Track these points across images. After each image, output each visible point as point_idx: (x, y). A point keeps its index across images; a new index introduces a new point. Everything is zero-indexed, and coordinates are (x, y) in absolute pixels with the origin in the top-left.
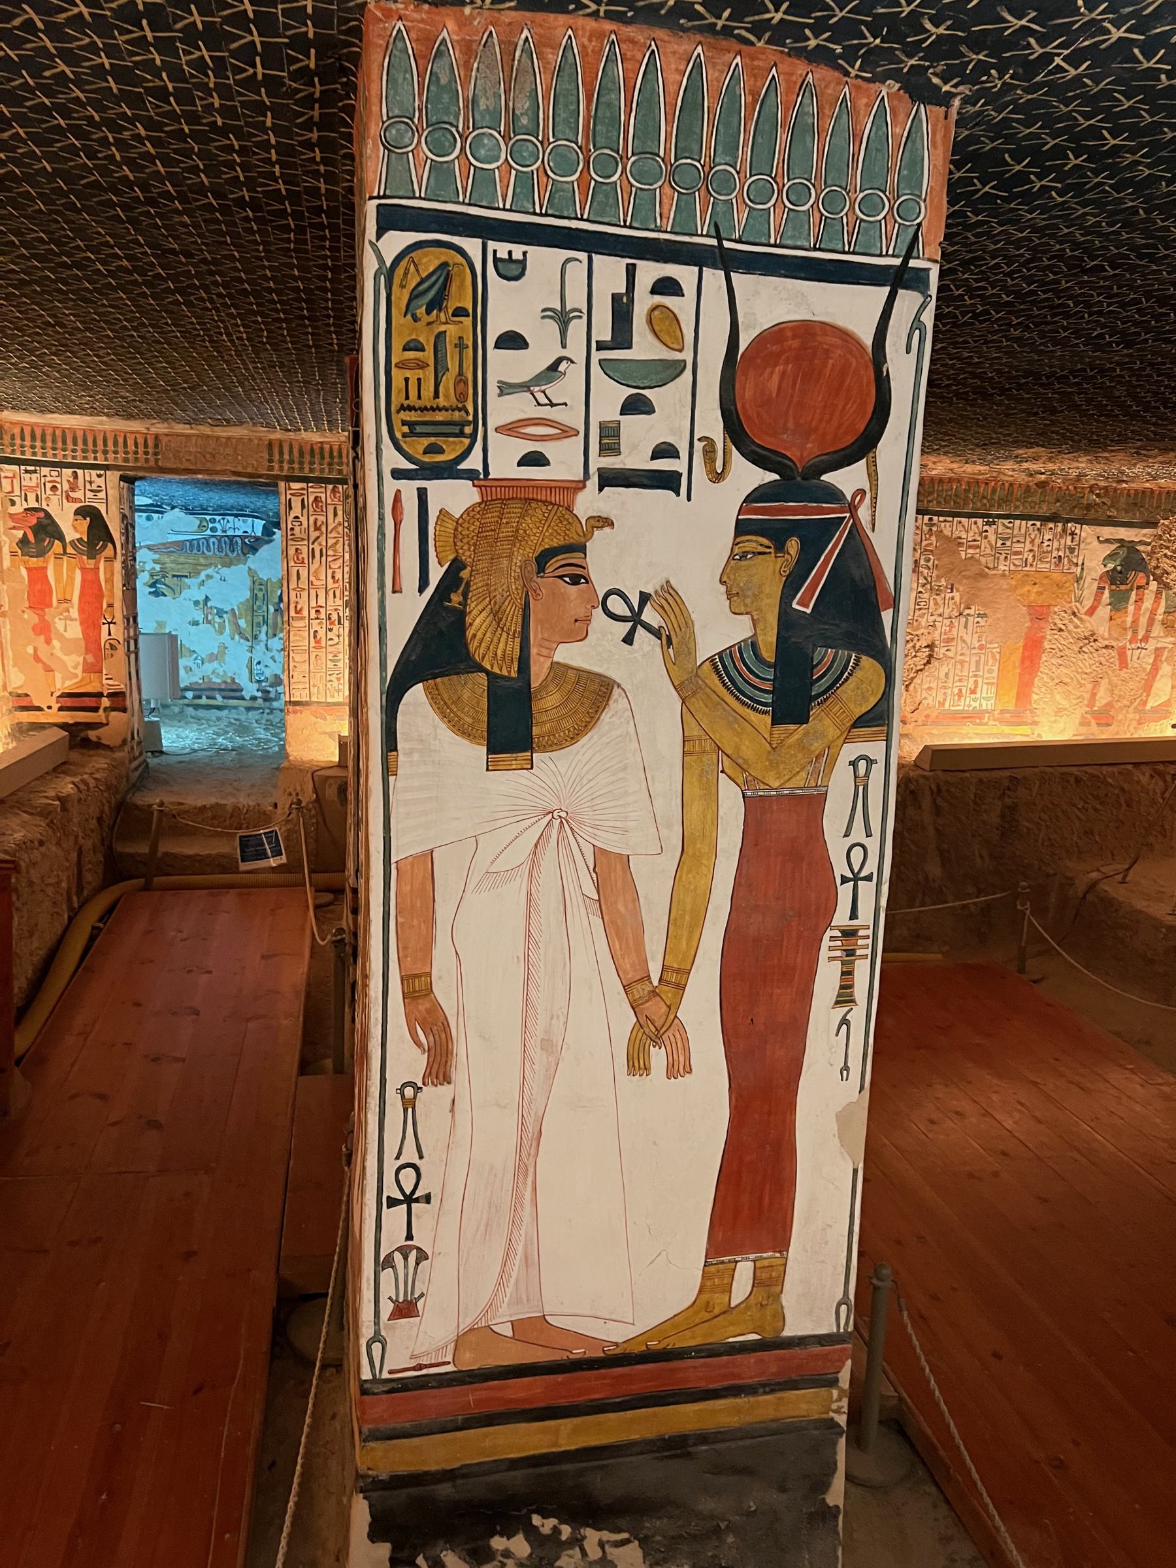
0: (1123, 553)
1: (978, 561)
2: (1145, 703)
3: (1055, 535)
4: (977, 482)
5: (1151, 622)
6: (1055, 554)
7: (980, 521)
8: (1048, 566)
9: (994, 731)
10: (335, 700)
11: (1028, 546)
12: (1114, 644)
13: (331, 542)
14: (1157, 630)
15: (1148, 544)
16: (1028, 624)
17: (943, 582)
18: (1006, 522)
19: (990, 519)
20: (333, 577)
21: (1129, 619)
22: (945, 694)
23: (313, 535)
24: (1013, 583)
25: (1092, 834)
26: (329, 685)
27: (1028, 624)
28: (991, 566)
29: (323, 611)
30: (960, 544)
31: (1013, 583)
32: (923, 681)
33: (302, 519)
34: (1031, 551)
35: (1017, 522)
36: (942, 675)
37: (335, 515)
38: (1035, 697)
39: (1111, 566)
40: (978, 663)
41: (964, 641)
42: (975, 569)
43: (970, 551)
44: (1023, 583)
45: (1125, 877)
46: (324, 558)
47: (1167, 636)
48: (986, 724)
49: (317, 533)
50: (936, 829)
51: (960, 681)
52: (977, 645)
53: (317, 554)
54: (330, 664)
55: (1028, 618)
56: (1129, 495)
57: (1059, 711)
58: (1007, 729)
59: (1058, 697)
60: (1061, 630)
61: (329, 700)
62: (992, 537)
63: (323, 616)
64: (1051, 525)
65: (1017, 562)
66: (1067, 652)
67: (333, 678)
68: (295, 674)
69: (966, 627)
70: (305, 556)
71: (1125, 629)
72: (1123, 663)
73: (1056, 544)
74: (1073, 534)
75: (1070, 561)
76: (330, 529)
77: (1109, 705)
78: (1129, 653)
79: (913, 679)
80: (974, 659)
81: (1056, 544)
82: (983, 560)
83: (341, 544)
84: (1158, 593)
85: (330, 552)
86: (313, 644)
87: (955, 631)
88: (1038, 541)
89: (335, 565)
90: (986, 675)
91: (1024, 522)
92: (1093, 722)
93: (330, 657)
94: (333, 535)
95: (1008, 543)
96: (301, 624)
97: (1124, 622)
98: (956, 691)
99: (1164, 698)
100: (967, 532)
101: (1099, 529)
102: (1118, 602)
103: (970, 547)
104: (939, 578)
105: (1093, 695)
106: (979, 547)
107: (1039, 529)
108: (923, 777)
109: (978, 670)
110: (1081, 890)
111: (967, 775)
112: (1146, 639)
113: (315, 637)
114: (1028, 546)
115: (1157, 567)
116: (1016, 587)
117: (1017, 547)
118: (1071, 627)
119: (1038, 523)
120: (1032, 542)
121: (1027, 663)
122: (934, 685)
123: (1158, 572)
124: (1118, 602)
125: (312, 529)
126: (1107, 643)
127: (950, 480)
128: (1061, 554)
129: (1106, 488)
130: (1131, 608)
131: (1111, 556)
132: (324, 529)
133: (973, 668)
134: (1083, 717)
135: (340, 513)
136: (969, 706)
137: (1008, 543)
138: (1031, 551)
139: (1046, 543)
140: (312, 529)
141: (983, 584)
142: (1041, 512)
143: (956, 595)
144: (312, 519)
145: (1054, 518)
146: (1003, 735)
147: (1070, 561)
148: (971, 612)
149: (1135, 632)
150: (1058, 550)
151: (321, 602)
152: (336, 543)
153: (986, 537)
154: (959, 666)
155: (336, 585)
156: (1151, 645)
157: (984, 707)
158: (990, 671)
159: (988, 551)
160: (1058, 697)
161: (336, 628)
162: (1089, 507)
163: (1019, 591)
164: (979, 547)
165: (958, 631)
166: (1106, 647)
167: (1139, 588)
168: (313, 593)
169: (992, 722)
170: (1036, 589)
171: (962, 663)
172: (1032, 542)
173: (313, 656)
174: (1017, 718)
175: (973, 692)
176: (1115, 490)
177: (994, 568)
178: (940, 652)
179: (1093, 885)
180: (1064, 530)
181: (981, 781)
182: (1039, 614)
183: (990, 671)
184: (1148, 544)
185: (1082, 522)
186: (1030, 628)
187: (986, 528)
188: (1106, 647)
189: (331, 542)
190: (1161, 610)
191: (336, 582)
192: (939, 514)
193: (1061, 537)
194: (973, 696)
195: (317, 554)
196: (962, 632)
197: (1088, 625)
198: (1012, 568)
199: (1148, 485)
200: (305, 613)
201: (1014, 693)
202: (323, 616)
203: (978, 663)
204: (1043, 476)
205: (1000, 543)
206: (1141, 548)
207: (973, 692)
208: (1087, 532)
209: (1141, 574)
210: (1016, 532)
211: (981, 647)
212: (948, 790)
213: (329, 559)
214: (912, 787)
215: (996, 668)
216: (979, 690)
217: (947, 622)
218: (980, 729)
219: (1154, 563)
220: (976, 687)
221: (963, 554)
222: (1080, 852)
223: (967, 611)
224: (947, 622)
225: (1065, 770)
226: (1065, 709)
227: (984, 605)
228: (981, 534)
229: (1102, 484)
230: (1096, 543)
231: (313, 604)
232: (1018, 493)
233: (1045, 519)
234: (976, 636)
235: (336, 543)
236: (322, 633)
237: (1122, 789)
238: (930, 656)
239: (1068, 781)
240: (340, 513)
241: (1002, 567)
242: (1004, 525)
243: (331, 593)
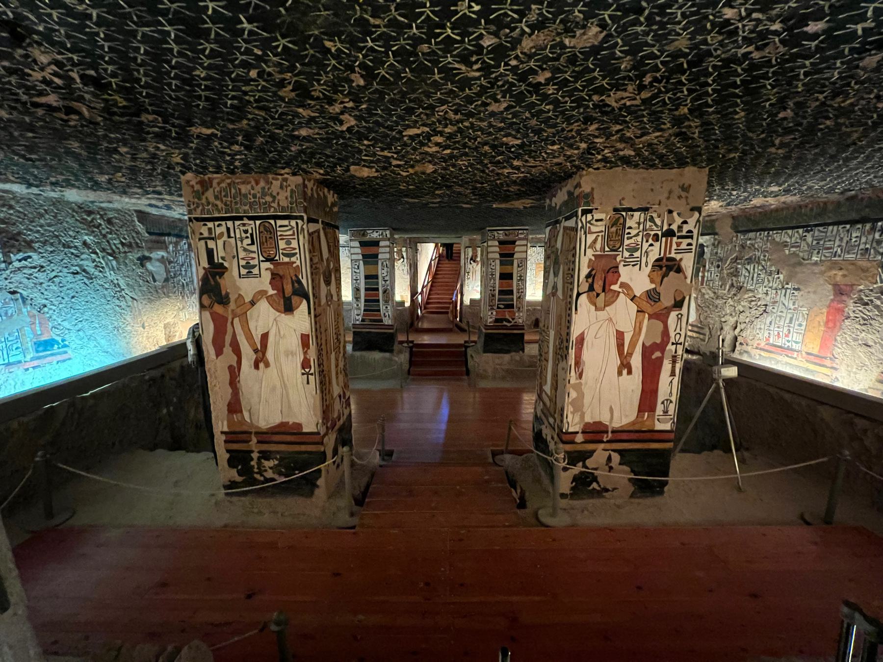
1: (798, 255)
3: (863, 233)
4: (800, 207)
6: (862, 246)
7: (801, 231)
8: (854, 256)
9: (801, 365)
16: (832, 297)
17: (773, 268)
18: (821, 228)
19: (808, 228)
24: (823, 268)
27: (832, 297)
28: (806, 257)
30: (786, 246)
31: (823, 268)
32: (758, 324)
34: (839, 246)
35: (830, 228)
36: (768, 322)
40: (791, 319)
42: (793, 260)
43: (794, 249)
44: (831, 269)
48: (795, 358)
52: (792, 307)
55: (832, 293)
58: (812, 367)
64: (860, 226)
65: (827, 255)
69: (785, 295)
73: (863, 239)
80: (789, 316)
82: (801, 254)
87: (778, 297)
88: (845, 239)
90: (796, 327)
91: (835, 228)
95: (822, 242)
100: (791, 238)
103: (793, 247)
104: (771, 266)
106: (799, 246)
107: (848, 231)
109: (791, 322)
114: (837, 243)
116: (825, 272)
117: (828, 244)
119: (848, 226)
120: (841, 240)
121: (831, 325)
122: (762, 327)
127: (782, 209)
128: (868, 246)
133: (788, 321)
137: (822, 242)
138: (839, 246)
139: (854, 240)
141: (798, 269)
142: (850, 218)
143: (781, 276)
145: (863, 221)
146: (807, 370)
148: (789, 286)
150: (866, 243)
153: (805, 240)
158: (800, 325)
159: (806, 248)
164: (799, 246)
165: (780, 298)
170: (840, 273)
171: (780, 317)
172: (841, 240)
174: (818, 359)
175: (787, 336)
178: (769, 308)
183: (800, 325)
192: (773, 230)
193: (869, 233)
196: (783, 298)
198: (823, 258)
203: (791, 319)
204: (853, 192)
205: (815, 242)
207: (787, 336)
210: (829, 234)
215: (804, 324)
216: (791, 335)
217: (774, 292)
220: (789, 332)
221: (787, 252)
223: (786, 286)
224: (774, 292)
227: (799, 283)
228: (801, 239)
232: (830, 207)
233: (853, 223)
238: (765, 311)
241: (815, 258)
242: (819, 230)
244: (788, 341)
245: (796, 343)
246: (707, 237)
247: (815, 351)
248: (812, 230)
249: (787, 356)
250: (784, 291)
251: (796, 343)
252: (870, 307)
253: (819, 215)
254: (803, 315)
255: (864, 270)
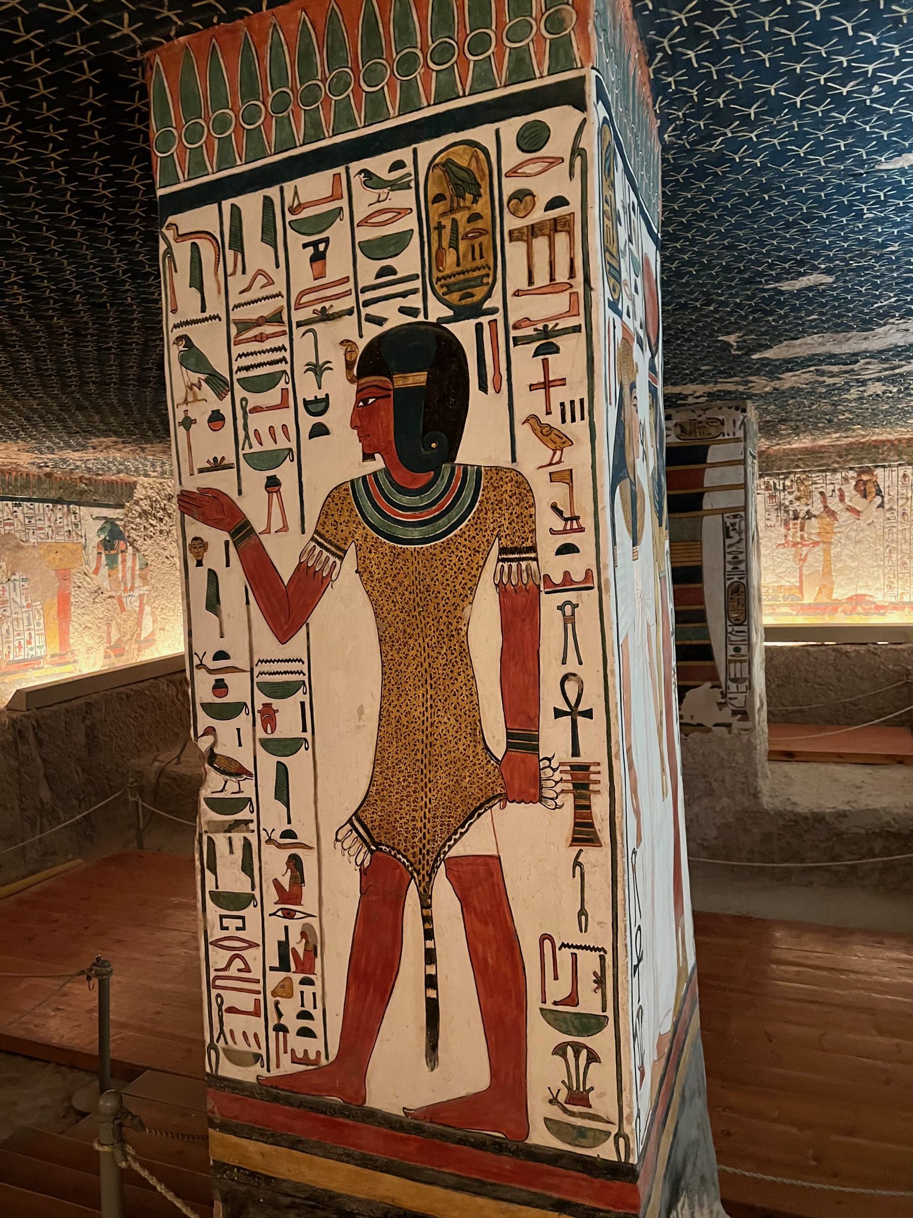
0: (108, 526)
1: (14, 536)
2: (139, 635)
5: (133, 578)
6: (66, 529)
7: (10, 503)
11: (47, 524)
12: (114, 594)
14: (138, 582)
15: (122, 520)
18: (28, 504)
19: (18, 502)
21: (120, 575)
22: (9, 647)
24: (42, 552)
25: (143, 735)
27: (57, 584)
31: (42, 552)
35: (36, 504)
38: (72, 641)
39: (102, 536)
40: (28, 618)
41: (16, 602)
42: (12, 543)
43: (7, 528)
45: (179, 760)
47: (144, 585)
48: (43, 668)
50: (42, 758)
51: (19, 635)
52: (25, 604)
56: (104, 485)
57: (89, 650)
58: (57, 670)
59: (86, 639)
60: (79, 587)
62: (21, 517)
64: (60, 506)
65: (42, 536)
66: (87, 603)
69: (15, 590)
71: (119, 583)
72: (123, 609)
74: (74, 513)
75: (77, 534)
77: (119, 640)
78: (124, 600)
80: (25, 615)
81: (65, 522)
82: (17, 535)
84: (134, 555)
87: (7, 594)
88: (53, 519)
90: (36, 628)
92: (112, 654)
95: (33, 521)
97: (117, 577)
98: (17, 643)
99: (150, 630)
101: (91, 509)
102: (112, 562)
105: (109, 634)
106: (12, 524)
108: (25, 716)
109: (30, 624)
110: (153, 778)
111: (53, 708)
112: (132, 589)
114: (47, 524)
115: (129, 537)
118: (85, 584)
119: (51, 505)
120: (49, 519)
121: (62, 615)
123: (131, 540)
124: (112, 562)
126: (110, 594)
129: (89, 479)
130: (120, 567)
131: (102, 529)
133: (26, 624)
134: (105, 651)
136: (28, 655)
139: (59, 520)
141: (21, 554)
147: (77, 534)
148: (17, 577)
149: (125, 584)
153: (16, 517)
154: (15, 623)
156: (137, 593)
157: (39, 654)
159: (20, 528)
160: (86, 639)
162: (82, 493)
163: (46, 560)
166: (110, 597)
167: (122, 552)
169: (46, 666)
170: (58, 556)
171: (17, 619)
172: (49, 519)
174: (61, 658)
175: (29, 643)
176: (96, 480)
177: (27, 541)
179: (162, 771)
180: (69, 510)
181: (67, 711)
182: (64, 575)
183: (39, 624)
184: (122, 520)
185: (79, 504)
186: (60, 587)
187: (15, 509)
188: (110, 597)
190: (137, 567)
194: (29, 646)
196: (13, 594)
197: (95, 581)
198: (39, 540)
199: (113, 478)
201: (57, 639)
203: (28, 618)
205: (27, 521)
206: (118, 523)
208: (83, 511)
209: (122, 542)
211: (29, 606)
212: (45, 723)
214: (19, 726)
215: (42, 621)
216: (33, 640)
218: (38, 673)
219: (126, 534)
220: (31, 638)
222: (139, 751)
223: (13, 577)
225: (118, 690)
226: (92, 648)
229: (87, 476)
230: (91, 519)
232: (34, 481)
234: (23, 597)
237: (155, 698)
239: (122, 699)
241: (32, 540)
244: (31, 649)
245: (40, 647)
247: (57, 650)
248: (20, 505)
249: (33, 669)
250: (12, 584)
251: (40, 647)
252: (83, 590)
253: (25, 487)
254: (38, 612)
255: (73, 553)
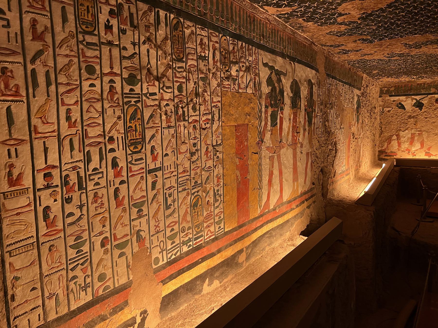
10: (82, 303)
13: (62, 62)
20: (68, 118)
23: (33, 47)
26: (72, 285)
29: (56, 173)
33: (9, 15)
37: (65, 19)
46: (53, 88)
49: (37, 46)
53: (41, 80)
54: (72, 253)
61: (73, 307)
63: (56, 181)
67: (78, 272)
68: (18, 292)
70: (21, 82)
76: (59, 39)
79: (334, 160)
83: (75, 67)
85: (62, 79)
86: (43, 230)
89: (71, 99)
93: (71, 241)
94: (64, 51)
96: (23, 201)
113: (46, 217)
125: (29, 37)
132: (48, 38)
135: (71, 17)
140: (29, 37)
144: (27, 19)
151: (53, 158)
152: (69, 65)
155: (73, 130)
161: (76, 196)
168: (38, 145)
173: (45, 250)
189: (62, 62)
191: (72, 125)
195: (41, 80)
200: (27, 182)
202: (56, 181)
213: (62, 89)
231: (40, 164)
235: (69, 65)
236: (56, 208)
240: (71, 17)
243: (66, 143)
246: (314, 72)
